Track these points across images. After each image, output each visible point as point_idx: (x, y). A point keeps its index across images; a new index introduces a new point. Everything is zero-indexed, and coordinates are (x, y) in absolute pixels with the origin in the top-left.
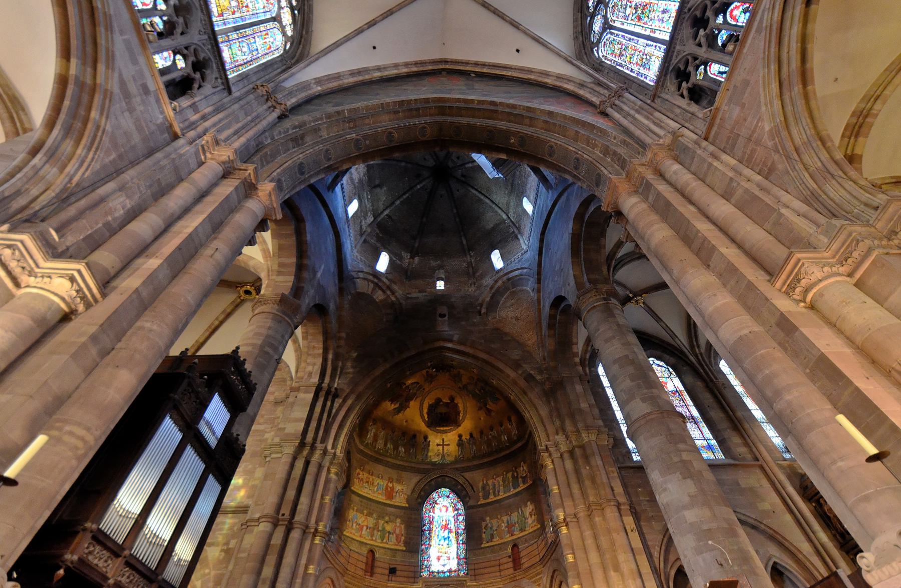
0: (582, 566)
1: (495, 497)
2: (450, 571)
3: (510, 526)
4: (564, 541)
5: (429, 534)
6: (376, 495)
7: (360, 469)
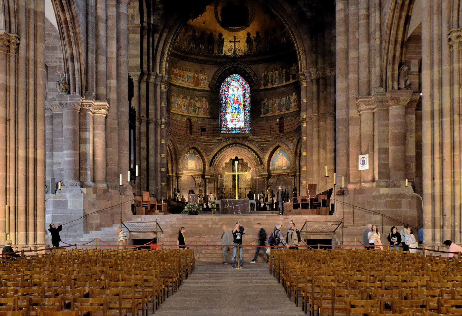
0: (309, 144)
1: (272, 84)
2: (240, 128)
3: (280, 105)
4: (303, 130)
5: (225, 105)
6: (187, 84)
7: (174, 67)
